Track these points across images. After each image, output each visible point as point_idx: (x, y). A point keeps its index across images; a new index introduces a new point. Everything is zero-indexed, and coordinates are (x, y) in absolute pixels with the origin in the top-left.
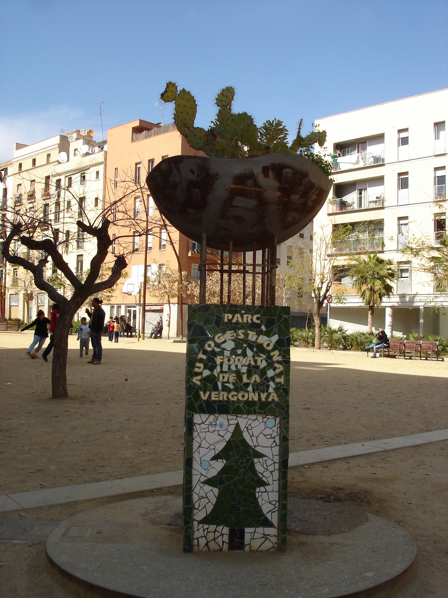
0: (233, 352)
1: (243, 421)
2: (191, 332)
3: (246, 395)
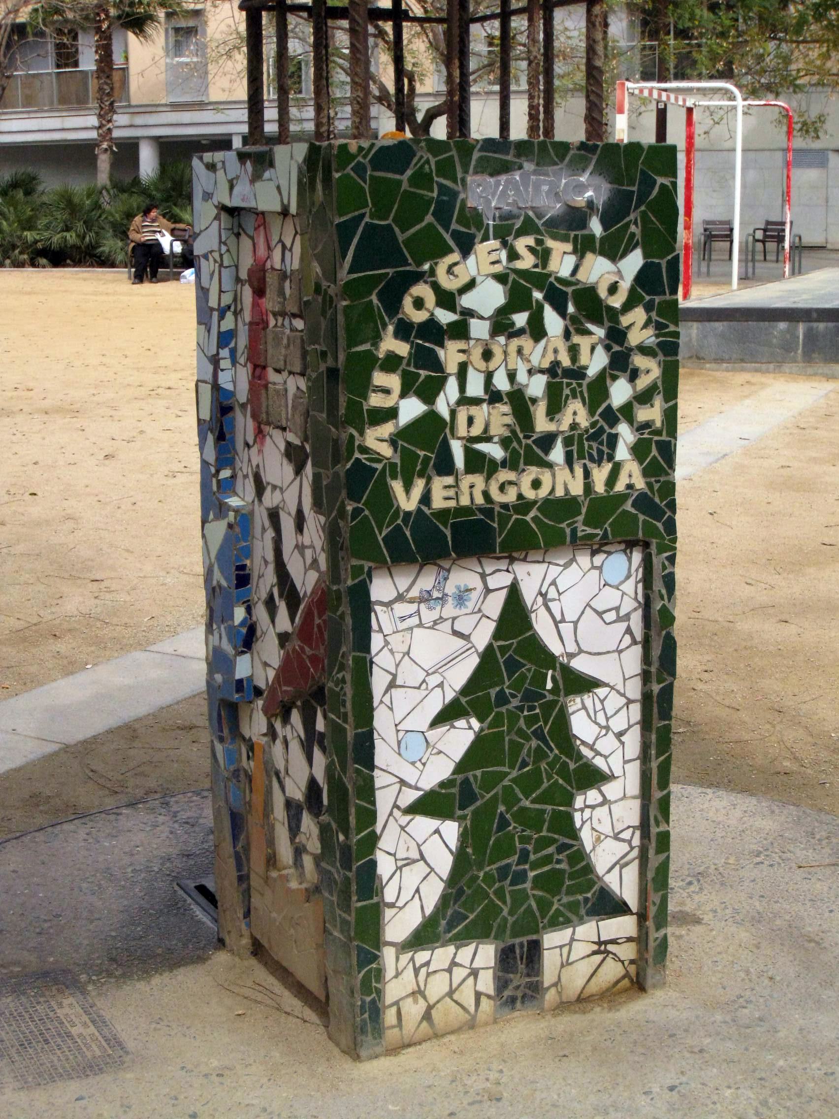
0: (501, 324)
1: (531, 577)
2: (458, 205)
3: (546, 478)
